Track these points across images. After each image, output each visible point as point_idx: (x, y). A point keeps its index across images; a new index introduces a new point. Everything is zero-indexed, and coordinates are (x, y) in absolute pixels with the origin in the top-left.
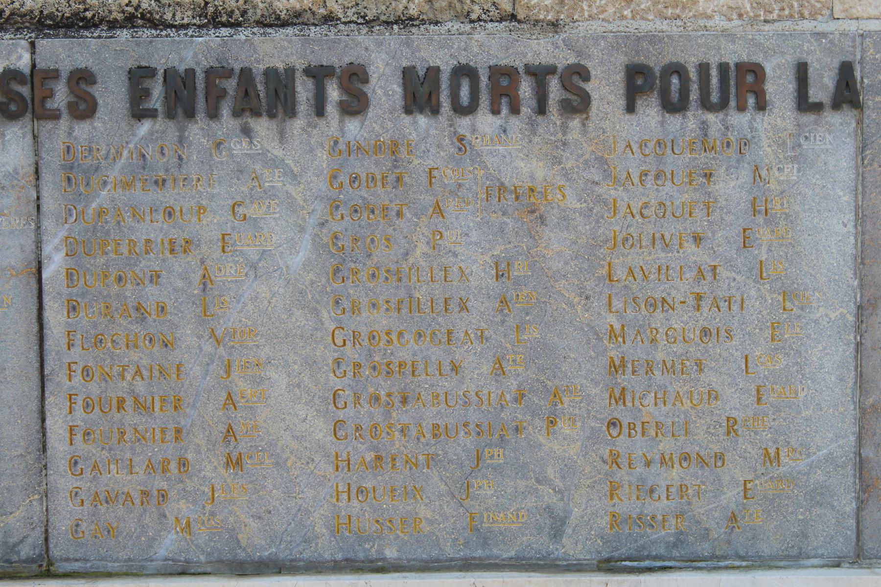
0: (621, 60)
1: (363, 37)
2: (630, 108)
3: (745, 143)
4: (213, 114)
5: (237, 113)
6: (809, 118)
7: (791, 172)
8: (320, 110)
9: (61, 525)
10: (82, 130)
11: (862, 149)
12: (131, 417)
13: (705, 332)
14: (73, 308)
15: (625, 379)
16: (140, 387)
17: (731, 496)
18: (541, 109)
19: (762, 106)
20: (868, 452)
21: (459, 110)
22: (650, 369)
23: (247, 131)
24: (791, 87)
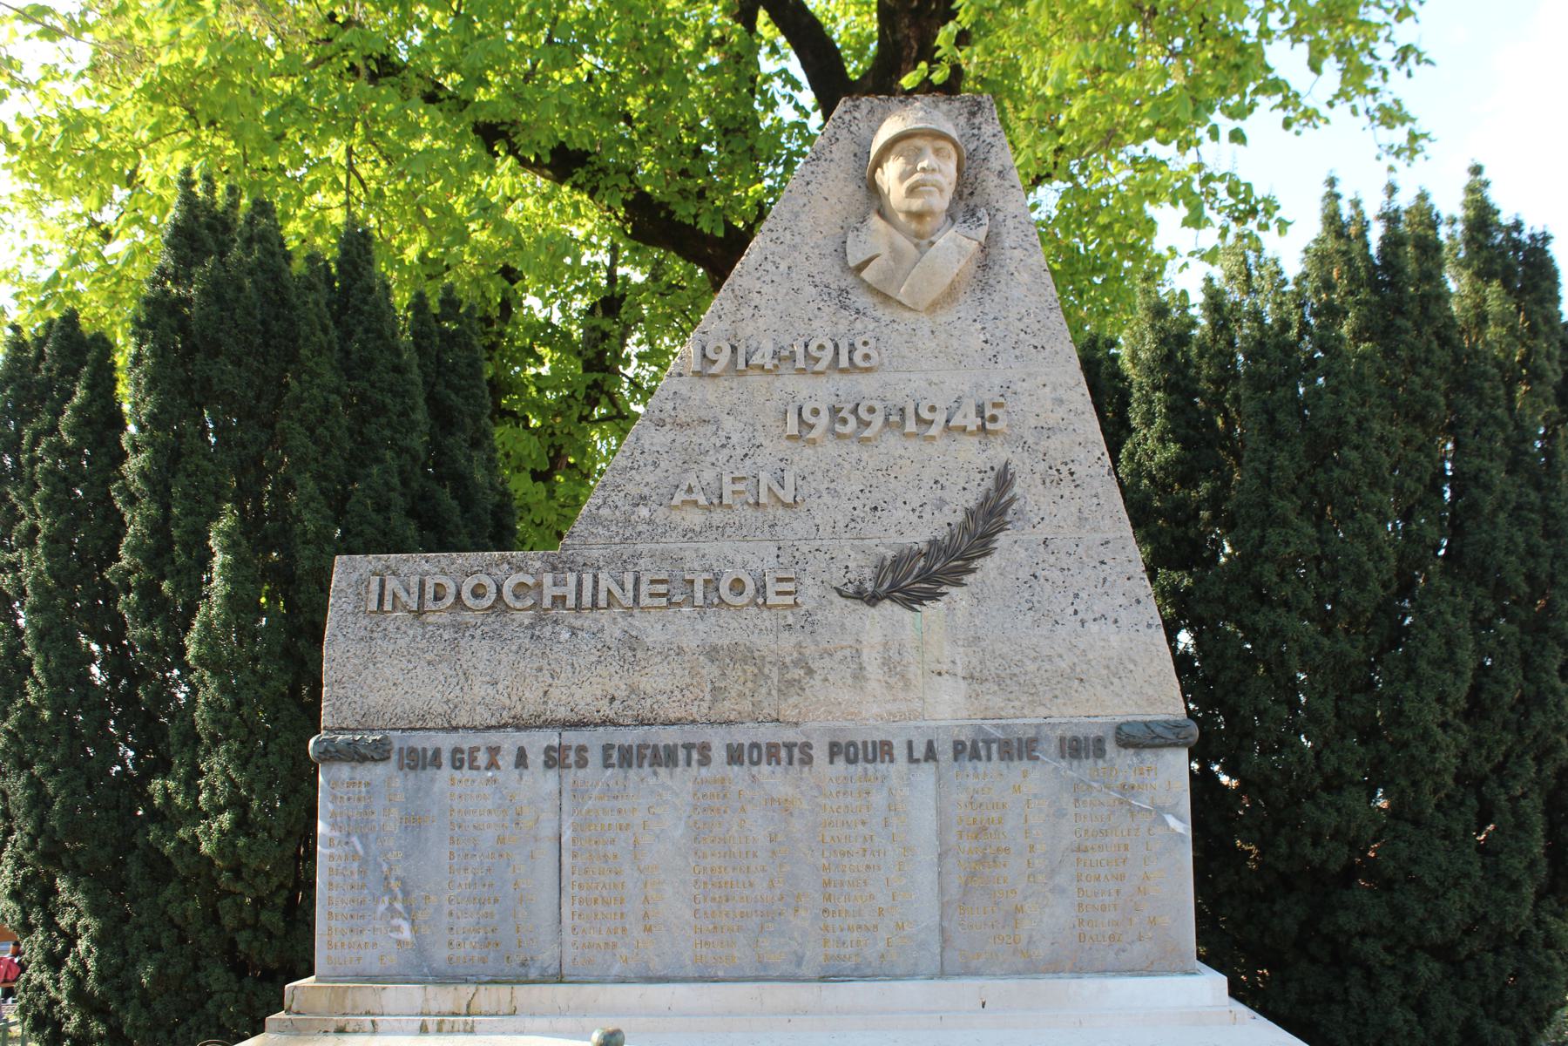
0: (827, 740)
1: (709, 730)
2: (831, 762)
3: (884, 777)
4: (640, 766)
5: (651, 765)
6: (914, 766)
7: (906, 791)
8: (689, 764)
9: (567, 960)
10: (581, 773)
11: (939, 779)
12: (600, 908)
13: (868, 867)
14: (574, 856)
15: (831, 890)
16: (605, 893)
17: (881, 945)
18: (790, 763)
19: (892, 761)
20: (945, 924)
21: (753, 763)
22: (842, 884)
23: (655, 773)
24: (906, 751)
